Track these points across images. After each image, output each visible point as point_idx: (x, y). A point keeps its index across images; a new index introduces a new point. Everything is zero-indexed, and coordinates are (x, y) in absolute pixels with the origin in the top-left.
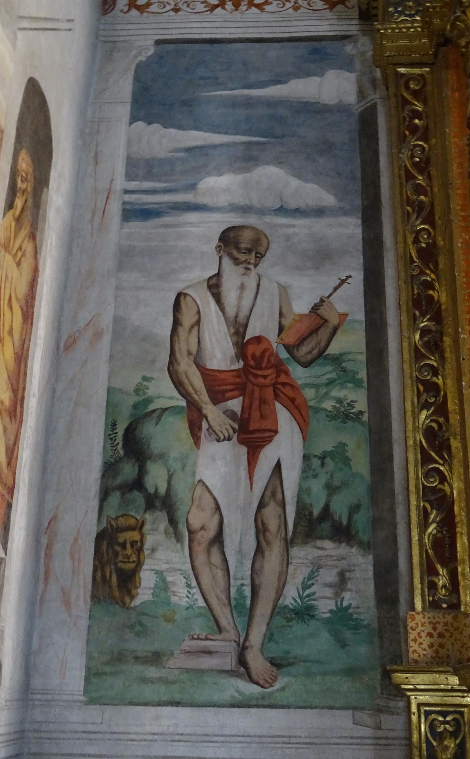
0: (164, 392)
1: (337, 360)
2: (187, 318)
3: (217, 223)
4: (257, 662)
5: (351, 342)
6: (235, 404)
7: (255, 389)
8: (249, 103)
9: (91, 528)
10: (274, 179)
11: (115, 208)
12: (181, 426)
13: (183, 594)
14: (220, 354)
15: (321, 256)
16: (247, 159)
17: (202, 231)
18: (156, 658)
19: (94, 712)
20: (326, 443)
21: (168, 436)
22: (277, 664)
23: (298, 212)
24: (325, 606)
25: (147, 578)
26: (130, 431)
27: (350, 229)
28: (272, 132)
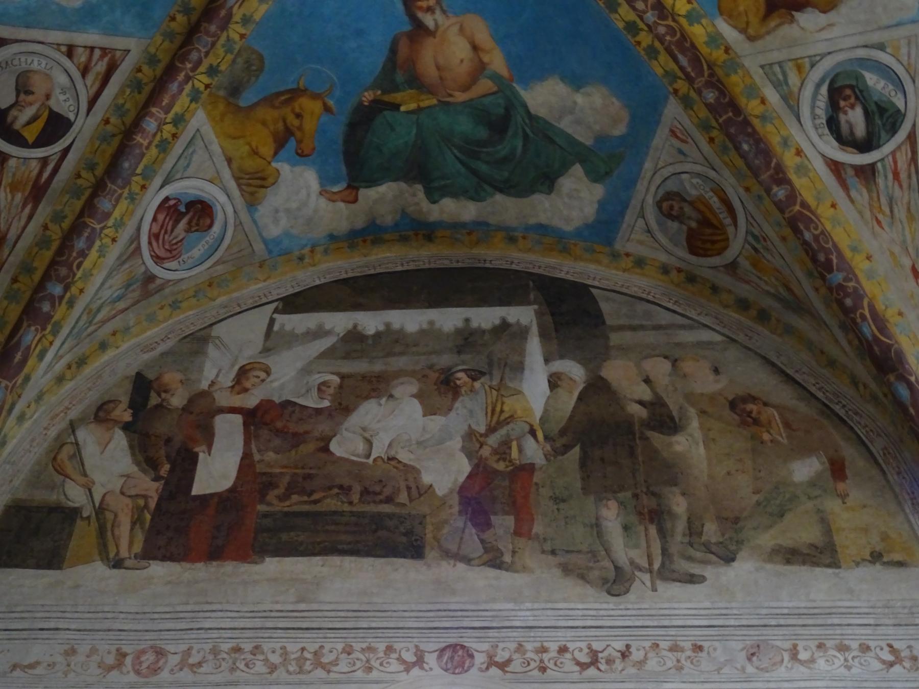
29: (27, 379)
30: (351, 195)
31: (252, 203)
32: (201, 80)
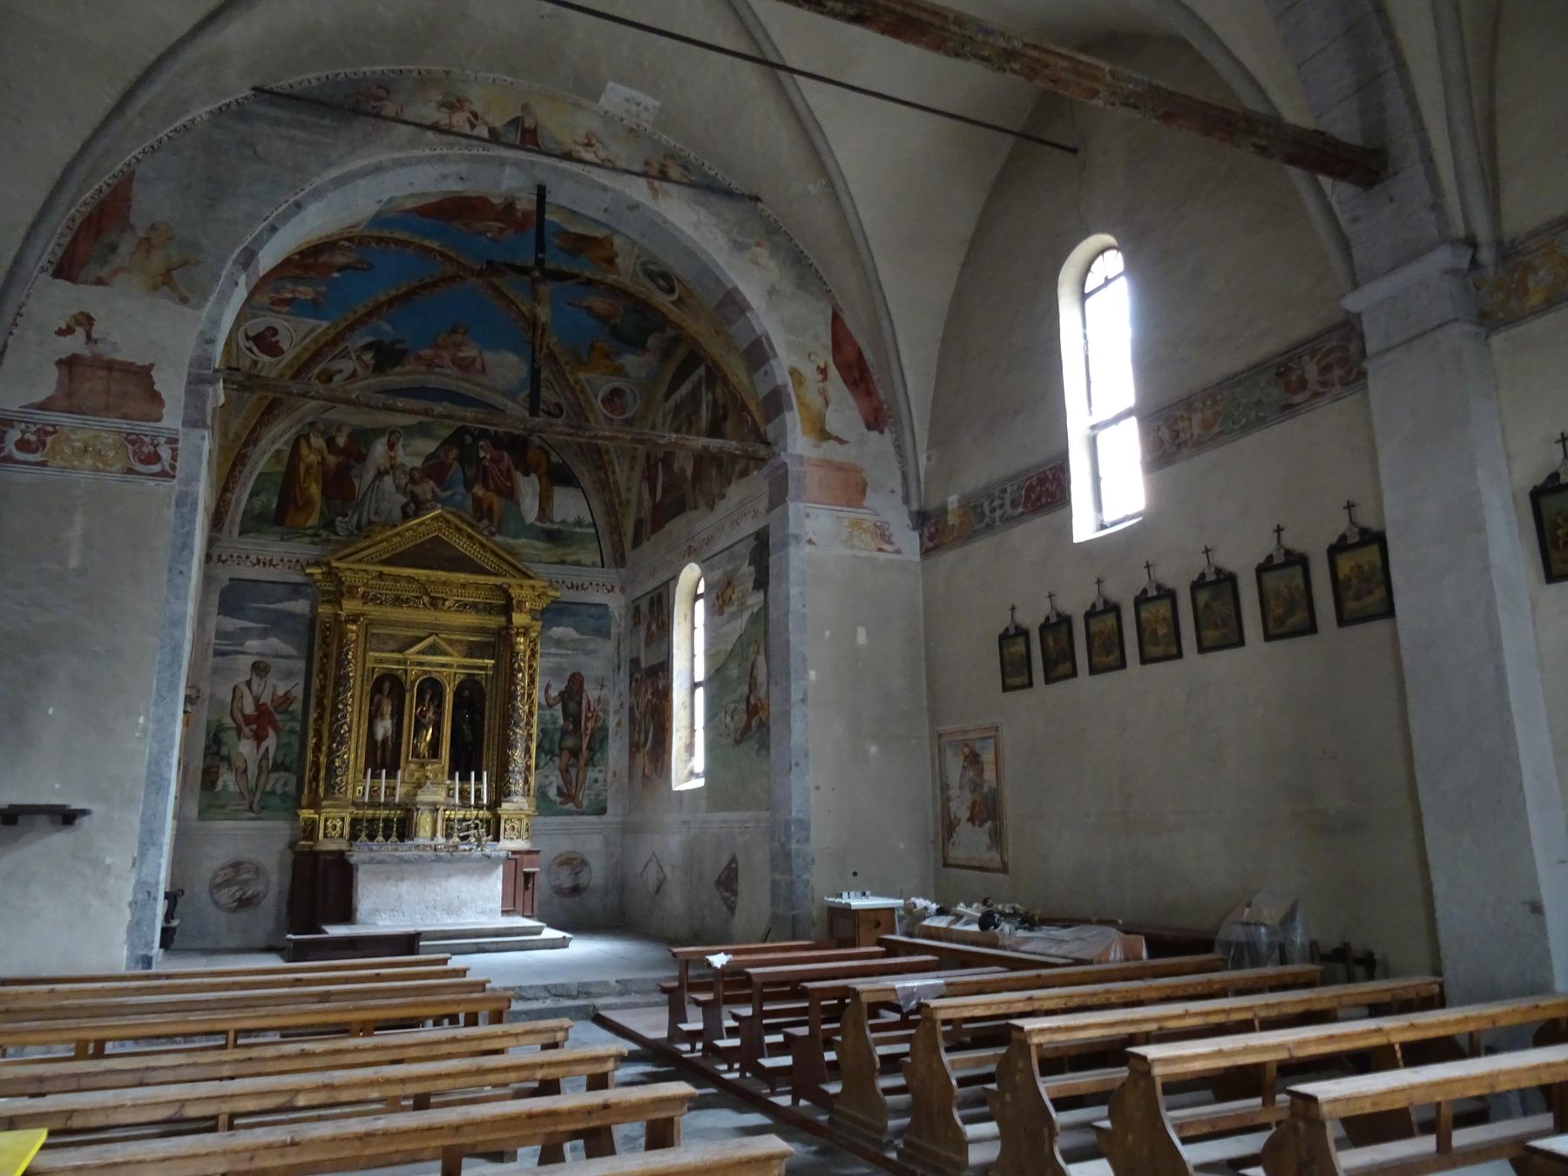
0: (228, 721)
1: (292, 713)
2: (238, 695)
3: (251, 660)
4: (255, 806)
5: (297, 707)
6: (254, 727)
7: (261, 721)
8: (266, 610)
9: (201, 766)
10: (274, 642)
11: (211, 651)
12: (234, 733)
13: (232, 787)
14: (249, 709)
15: (289, 674)
16: (263, 634)
17: (245, 662)
18: (222, 807)
19: (201, 824)
20: (285, 740)
21: (229, 737)
22: (263, 808)
23: (282, 657)
24: (279, 790)
25: (220, 783)
26: (216, 735)
27: (300, 665)
28: (276, 623)
29: (616, 482)
30: (648, 350)
32: (568, 368)
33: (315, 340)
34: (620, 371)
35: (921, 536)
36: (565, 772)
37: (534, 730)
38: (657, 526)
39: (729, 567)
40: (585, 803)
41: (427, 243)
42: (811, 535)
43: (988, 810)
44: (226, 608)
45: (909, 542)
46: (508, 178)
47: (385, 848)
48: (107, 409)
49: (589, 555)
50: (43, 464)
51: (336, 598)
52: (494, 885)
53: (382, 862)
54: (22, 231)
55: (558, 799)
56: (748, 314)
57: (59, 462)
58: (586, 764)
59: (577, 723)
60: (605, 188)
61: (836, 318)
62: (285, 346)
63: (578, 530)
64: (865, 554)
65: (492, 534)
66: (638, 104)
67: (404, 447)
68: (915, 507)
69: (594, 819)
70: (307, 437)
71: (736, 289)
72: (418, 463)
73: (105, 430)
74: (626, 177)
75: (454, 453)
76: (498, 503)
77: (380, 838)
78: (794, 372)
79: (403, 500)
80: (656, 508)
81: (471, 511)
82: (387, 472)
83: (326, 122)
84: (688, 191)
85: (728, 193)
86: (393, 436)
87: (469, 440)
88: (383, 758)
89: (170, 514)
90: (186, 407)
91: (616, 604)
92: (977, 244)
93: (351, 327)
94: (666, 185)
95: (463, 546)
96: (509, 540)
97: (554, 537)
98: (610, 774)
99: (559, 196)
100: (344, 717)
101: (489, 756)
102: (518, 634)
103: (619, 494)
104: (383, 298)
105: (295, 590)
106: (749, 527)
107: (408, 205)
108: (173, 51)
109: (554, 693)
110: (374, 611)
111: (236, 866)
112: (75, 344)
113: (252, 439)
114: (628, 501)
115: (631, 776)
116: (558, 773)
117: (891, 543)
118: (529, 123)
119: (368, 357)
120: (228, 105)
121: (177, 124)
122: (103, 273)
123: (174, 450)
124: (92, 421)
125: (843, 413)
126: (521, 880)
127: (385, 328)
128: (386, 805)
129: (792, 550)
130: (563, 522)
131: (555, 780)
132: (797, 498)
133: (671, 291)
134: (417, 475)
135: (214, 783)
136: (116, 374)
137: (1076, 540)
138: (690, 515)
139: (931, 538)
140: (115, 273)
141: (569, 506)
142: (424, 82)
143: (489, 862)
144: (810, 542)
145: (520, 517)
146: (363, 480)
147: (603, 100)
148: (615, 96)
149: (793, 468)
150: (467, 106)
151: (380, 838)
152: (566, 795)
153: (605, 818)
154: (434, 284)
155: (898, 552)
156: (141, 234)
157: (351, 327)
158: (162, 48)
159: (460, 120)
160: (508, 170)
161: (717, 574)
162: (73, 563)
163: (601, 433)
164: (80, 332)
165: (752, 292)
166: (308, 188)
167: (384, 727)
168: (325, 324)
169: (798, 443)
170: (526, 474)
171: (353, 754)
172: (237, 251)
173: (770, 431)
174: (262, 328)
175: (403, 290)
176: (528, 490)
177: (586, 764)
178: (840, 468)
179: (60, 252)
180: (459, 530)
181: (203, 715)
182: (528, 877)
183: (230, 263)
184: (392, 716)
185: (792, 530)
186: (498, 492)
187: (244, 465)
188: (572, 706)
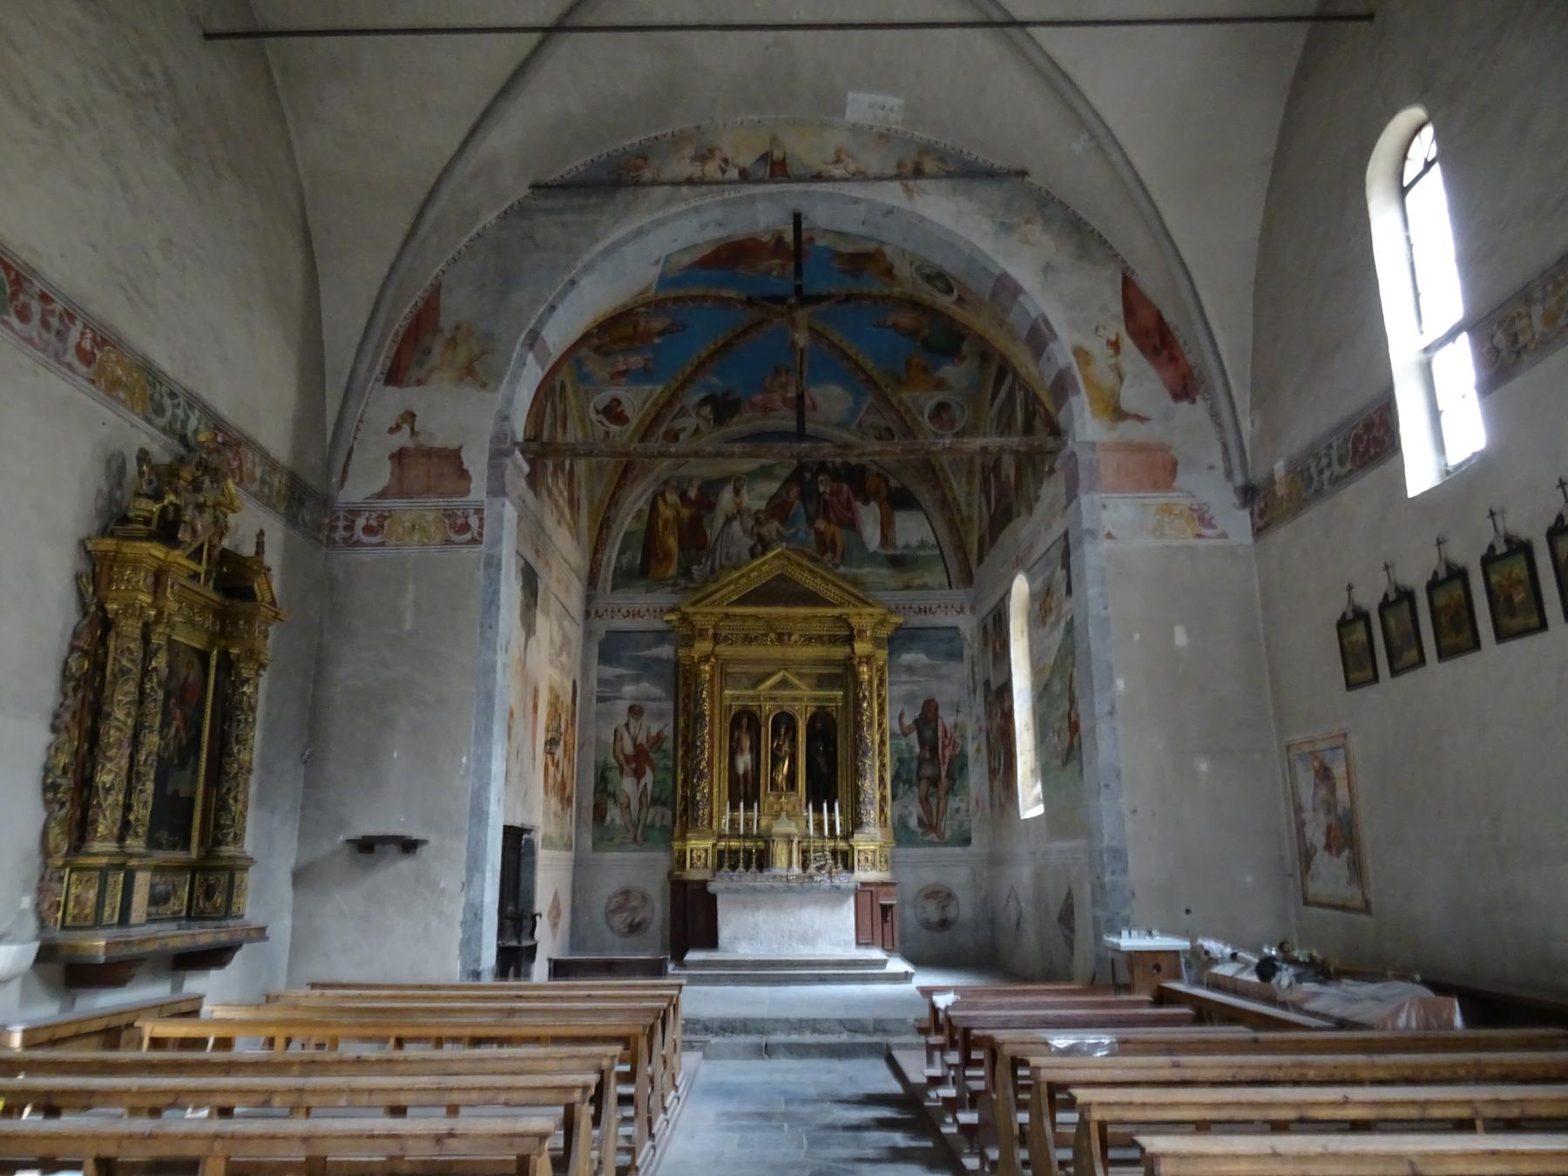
0: (612, 761)
5: (668, 745)
7: (639, 760)
8: (638, 657)
10: (646, 687)
14: (629, 748)
15: (660, 715)
16: (637, 679)
17: (622, 706)
21: (613, 775)
23: (653, 700)
24: (658, 824)
25: (608, 818)
27: (669, 706)
28: (647, 668)
29: (955, 499)
31: (949, 388)
32: (889, 390)
33: (654, 404)
34: (941, 384)
35: (1252, 514)
36: (924, 801)
37: (887, 760)
38: (993, 540)
39: (1047, 574)
40: (948, 834)
41: (724, 293)
42: (1109, 528)
43: (1344, 836)
44: (606, 657)
45: (1237, 523)
46: (763, 213)
47: (747, 878)
48: (428, 491)
49: (935, 577)
50: (382, 544)
51: (688, 641)
52: (846, 915)
53: (737, 891)
54: (353, 350)
55: (919, 830)
56: (1021, 298)
57: (393, 541)
58: (947, 793)
59: (934, 750)
60: (856, 201)
61: (1128, 285)
62: (629, 412)
63: (923, 553)
64: (1180, 542)
65: (836, 566)
66: (883, 108)
67: (749, 492)
68: (1239, 480)
69: (958, 850)
70: (663, 494)
71: (1005, 275)
72: (761, 505)
73: (423, 509)
74: (879, 184)
75: (795, 490)
76: (840, 536)
77: (741, 868)
78: (1079, 352)
79: (749, 542)
80: (993, 519)
81: (814, 545)
82: (734, 518)
83: (593, 201)
84: (945, 183)
85: (991, 174)
86: (738, 482)
87: (808, 476)
88: (744, 791)
89: (480, 574)
90: (489, 479)
91: (967, 625)
92: (1280, 161)
93: (682, 386)
94: (922, 183)
95: (808, 581)
96: (853, 570)
97: (898, 562)
98: (972, 804)
99: (820, 216)
100: (702, 753)
101: (843, 787)
102: (860, 663)
103: (959, 510)
104: (704, 354)
105: (660, 637)
106: (1057, 529)
107: (687, 260)
108: (447, 170)
109: (908, 721)
110: (724, 650)
111: (626, 893)
112: (403, 439)
113: (614, 502)
114: (970, 517)
115: (992, 805)
116: (916, 802)
117: (1214, 527)
118: (777, 155)
119: (707, 411)
120: (511, 207)
121: (472, 233)
122: (422, 374)
123: (481, 519)
124: (418, 502)
125: (1142, 385)
126: (878, 912)
127: (715, 381)
128: (746, 836)
129: (1088, 547)
130: (907, 546)
131: (914, 811)
132: (1092, 488)
133: (950, 290)
134: (762, 517)
135: (603, 818)
136: (435, 460)
137: (1410, 495)
138: (1016, 523)
139: (1262, 515)
140: (430, 372)
141: (912, 530)
142: (677, 140)
143: (838, 893)
144: (1109, 536)
145: (863, 546)
146: (713, 529)
147: (848, 112)
148: (862, 106)
149: (1083, 457)
150: (718, 155)
151: (741, 868)
152: (928, 825)
153: (969, 849)
154: (746, 331)
155: (1224, 535)
156: (448, 335)
157: (682, 386)
158: (439, 170)
159: (712, 169)
160: (761, 206)
161: (1039, 582)
162: (408, 626)
163: (869, 449)
164: (406, 427)
165: (1024, 274)
166: (579, 265)
167: (744, 762)
168: (659, 388)
169: (1086, 426)
170: (866, 502)
171: (715, 787)
172: (523, 336)
173: (1061, 418)
174: (607, 402)
175: (721, 342)
176: (869, 518)
177: (947, 793)
178: (1142, 448)
179: (388, 363)
180: (800, 565)
181: (591, 757)
182: (886, 909)
183: (518, 347)
184: (751, 750)
185: (1086, 524)
186: (840, 523)
187: (609, 527)
188: (928, 733)
